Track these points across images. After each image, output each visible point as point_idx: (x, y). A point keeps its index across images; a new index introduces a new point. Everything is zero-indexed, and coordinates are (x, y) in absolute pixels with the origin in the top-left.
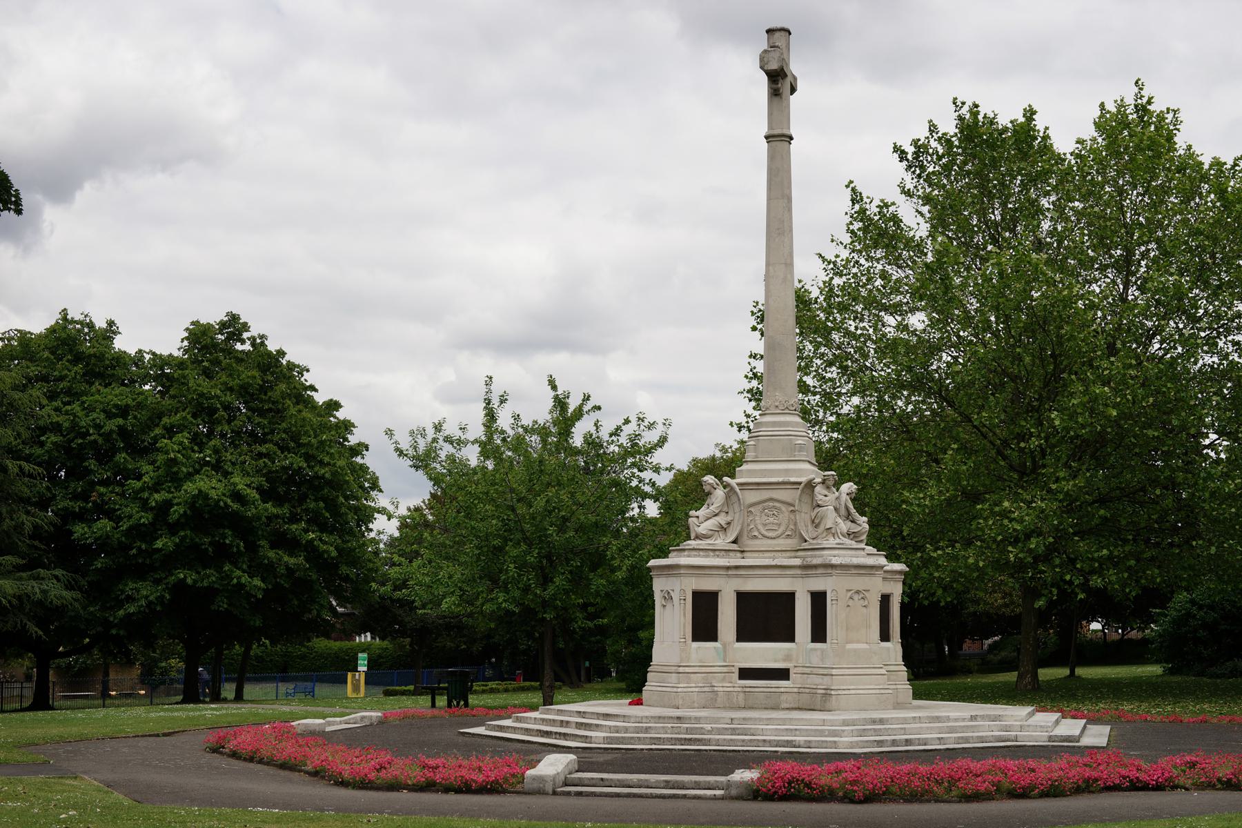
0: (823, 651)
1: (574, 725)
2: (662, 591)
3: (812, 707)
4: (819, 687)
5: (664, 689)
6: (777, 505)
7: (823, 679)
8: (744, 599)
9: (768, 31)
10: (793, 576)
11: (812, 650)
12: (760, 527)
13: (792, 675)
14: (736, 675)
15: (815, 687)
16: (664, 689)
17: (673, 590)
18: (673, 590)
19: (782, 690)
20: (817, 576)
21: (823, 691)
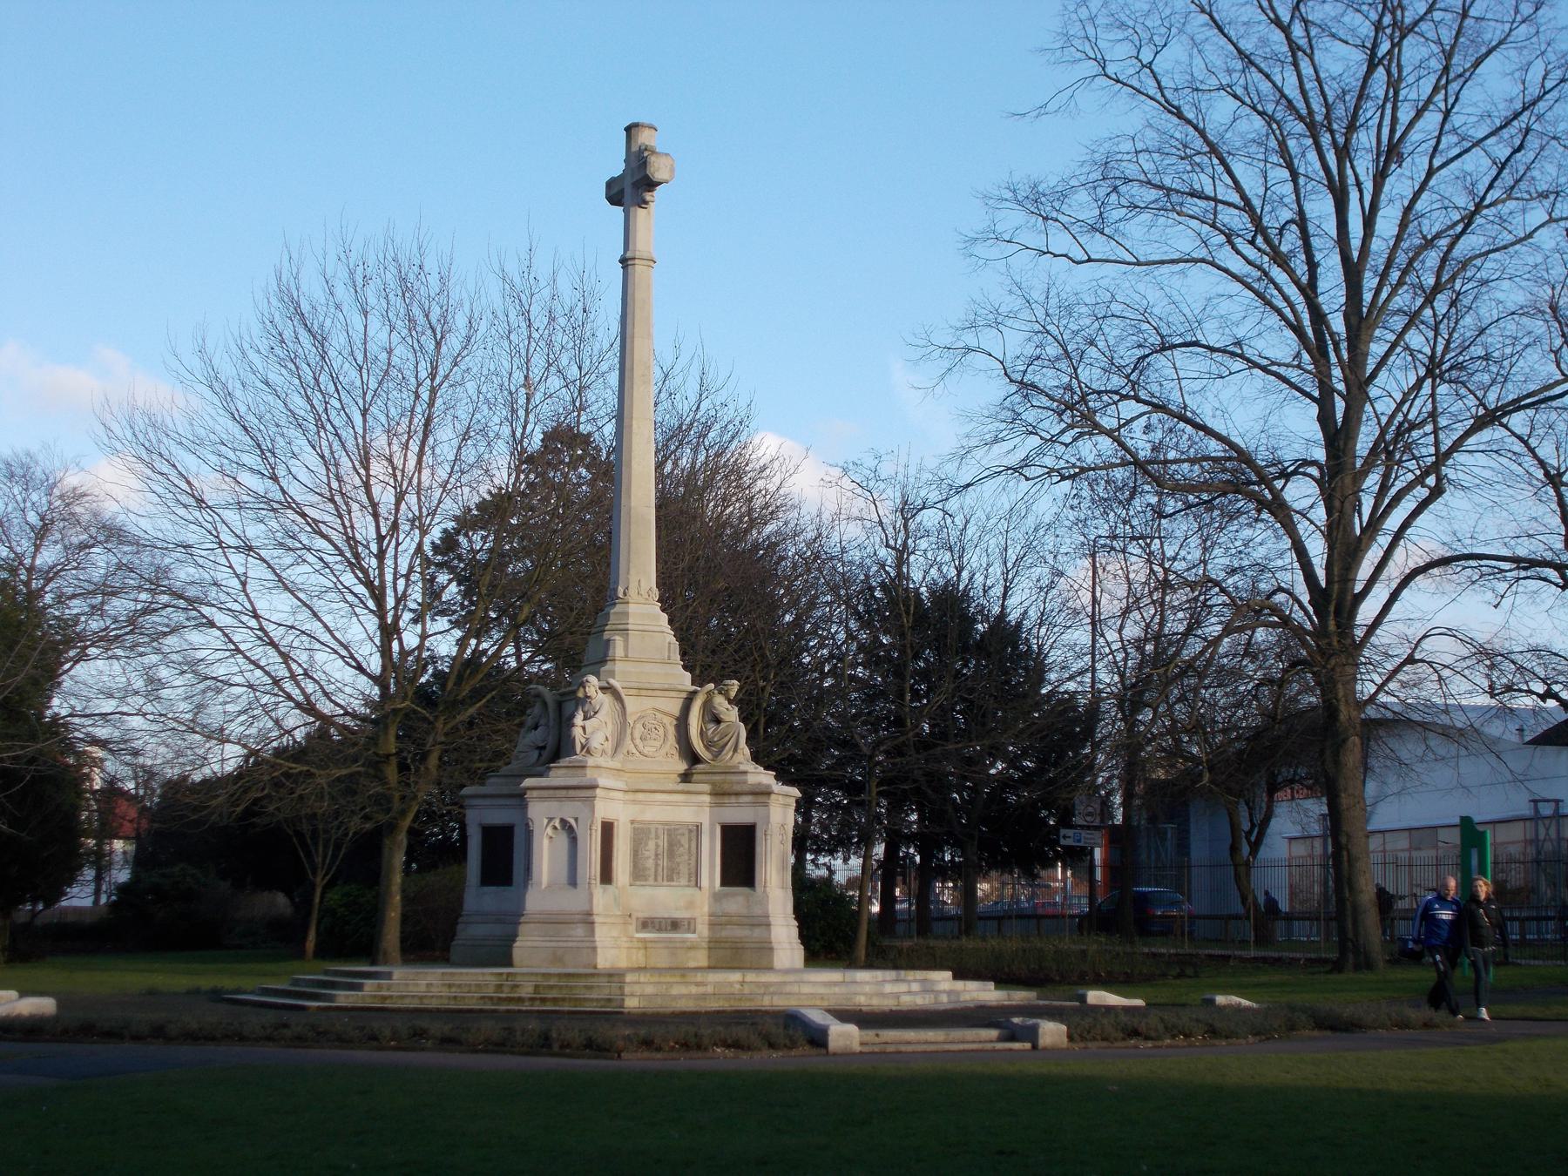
5: (561, 944)
8: (640, 834)
9: (628, 129)
10: (700, 805)
12: (638, 741)
14: (632, 928)
16: (561, 944)
17: (576, 820)
20: (740, 805)
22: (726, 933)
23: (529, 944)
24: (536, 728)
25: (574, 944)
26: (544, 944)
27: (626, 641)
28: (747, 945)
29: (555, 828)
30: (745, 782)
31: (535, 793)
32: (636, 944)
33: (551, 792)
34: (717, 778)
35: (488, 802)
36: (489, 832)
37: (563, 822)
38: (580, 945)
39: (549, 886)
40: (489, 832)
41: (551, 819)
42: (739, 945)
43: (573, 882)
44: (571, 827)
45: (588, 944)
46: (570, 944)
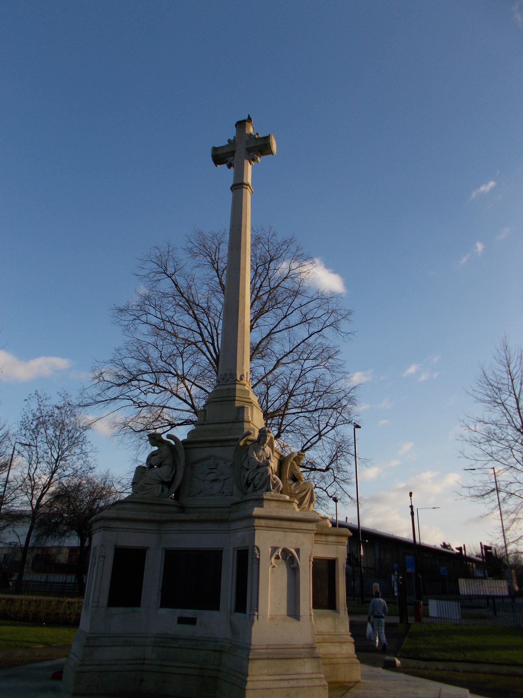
5: (292, 683)
16: (292, 683)
18: (298, 551)
20: (327, 543)
25: (305, 683)
26: (277, 684)
27: (252, 410)
28: (341, 661)
29: (277, 558)
31: (263, 522)
33: (277, 522)
35: (125, 525)
37: (285, 552)
38: (310, 683)
39: (272, 618)
41: (274, 549)
42: (335, 661)
44: (292, 558)
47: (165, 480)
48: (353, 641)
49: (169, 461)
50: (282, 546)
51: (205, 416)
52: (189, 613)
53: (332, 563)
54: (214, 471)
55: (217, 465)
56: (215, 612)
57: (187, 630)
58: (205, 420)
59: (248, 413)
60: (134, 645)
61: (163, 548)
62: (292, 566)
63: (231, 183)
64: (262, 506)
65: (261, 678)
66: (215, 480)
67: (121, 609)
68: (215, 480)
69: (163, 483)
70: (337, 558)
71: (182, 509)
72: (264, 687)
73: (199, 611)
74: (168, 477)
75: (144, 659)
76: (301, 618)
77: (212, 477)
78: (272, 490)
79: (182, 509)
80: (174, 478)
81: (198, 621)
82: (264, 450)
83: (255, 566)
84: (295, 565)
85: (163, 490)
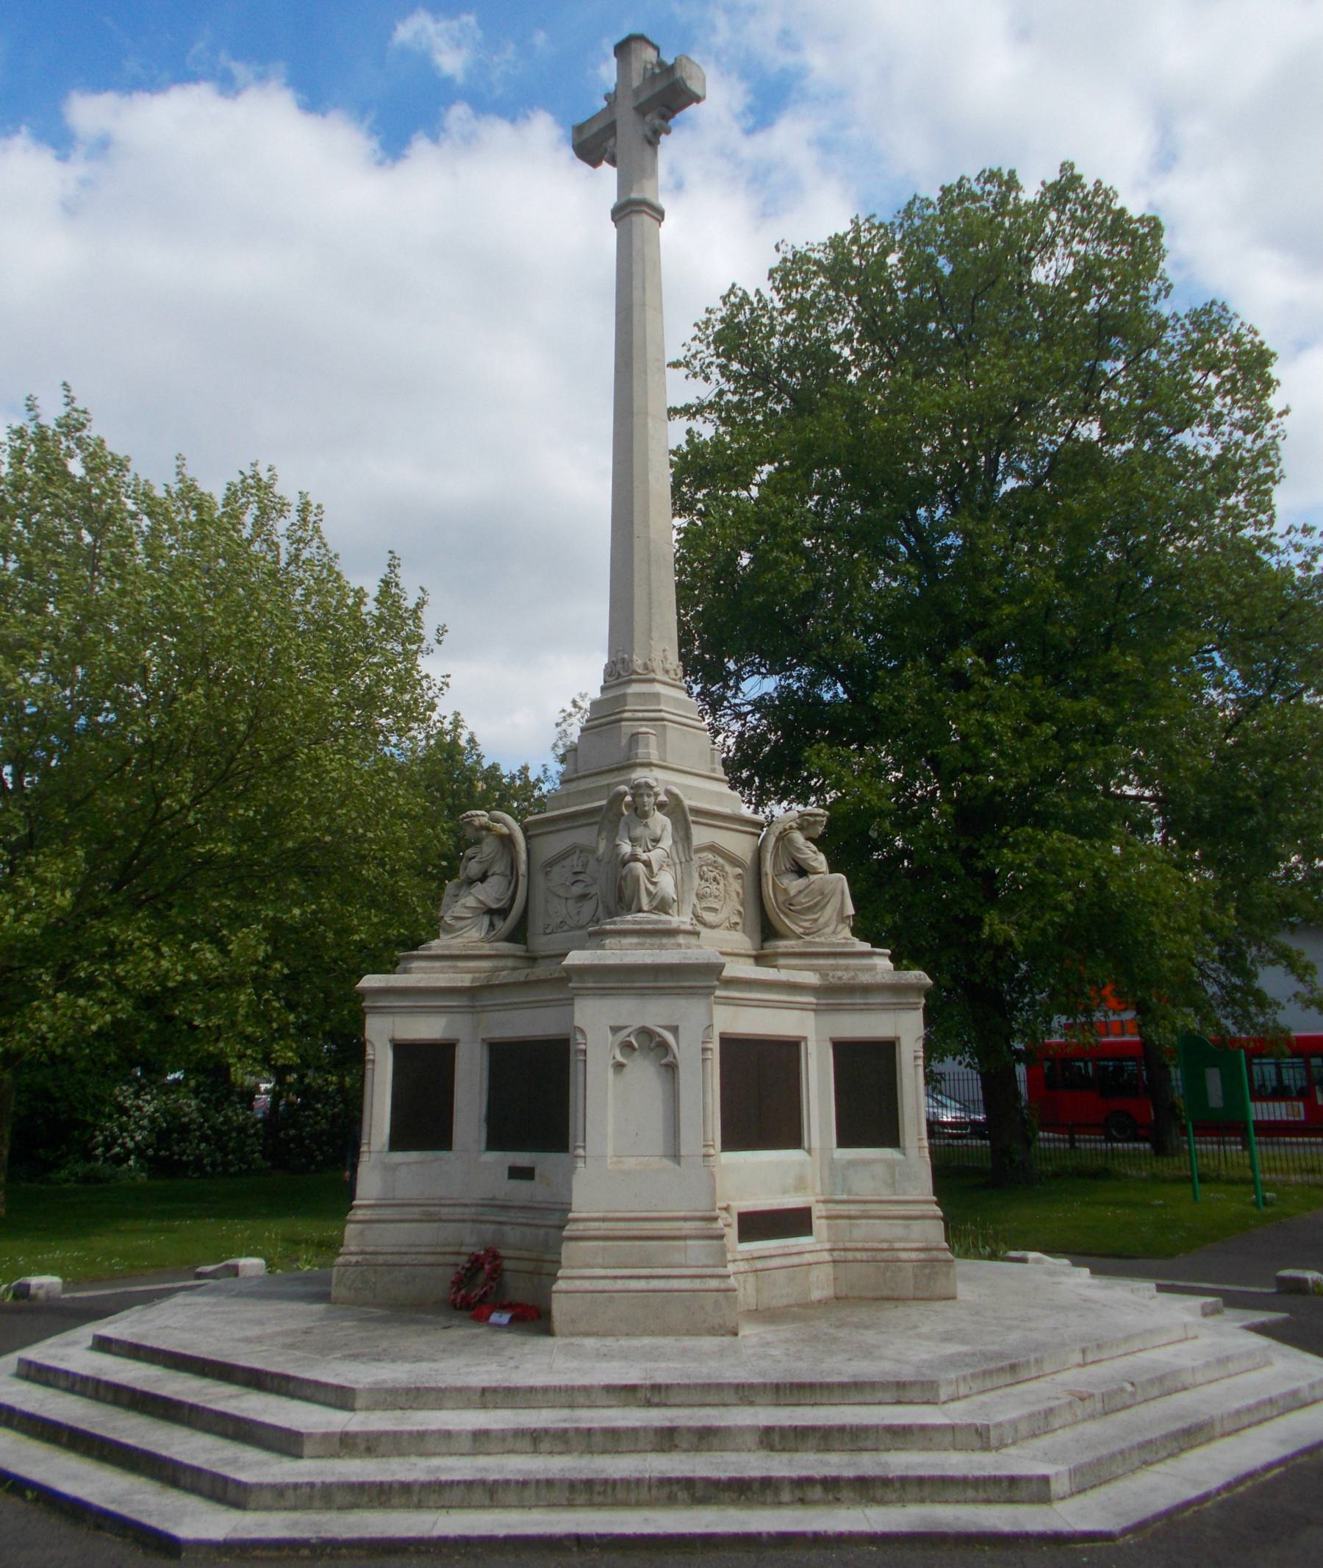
0: (891, 1165)
1: (751, 1440)
2: (615, 1030)
3: (886, 1293)
4: (897, 1245)
6: (720, 860)
7: (907, 1227)
10: (803, 1008)
11: (852, 1163)
13: (817, 1223)
14: (733, 1233)
15: (885, 1245)
17: (674, 1030)
18: (674, 1030)
19: (808, 1258)
20: (867, 1008)
21: (922, 1256)
22: (863, 1232)
23: (587, 1285)
24: (483, 878)
28: (904, 1255)
30: (872, 968)
32: (742, 1266)
34: (821, 962)
36: (405, 1052)
37: (645, 1033)
38: (697, 1284)
40: (405, 1052)
43: (676, 1156)
44: (664, 1047)
45: (714, 1283)
46: (675, 1284)
47: (495, 906)
48: (940, 1213)
49: (498, 868)
50: (637, 1024)
51: (576, 763)
52: (522, 1158)
53: (885, 1051)
54: (581, 877)
55: (585, 865)
56: (562, 1155)
57: (521, 1190)
58: (576, 771)
59: (647, 746)
60: (440, 1220)
61: (483, 1040)
62: (664, 1061)
63: (611, 199)
64: (603, 947)
65: (588, 1272)
66: (583, 897)
67: (413, 1156)
68: (583, 897)
69: (490, 912)
70: (898, 1038)
71: (532, 959)
72: (591, 1288)
73: (542, 1155)
74: (499, 900)
75: (462, 1245)
76: (682, 1160)
77: (577, 890)
78: (645, 908)
79: (532, 959)
80: (513, 899)
81: (537, 1172)
82: (646, 825)
83: (581, 1065)
84: (669, 1059)
85: (492, 925)
